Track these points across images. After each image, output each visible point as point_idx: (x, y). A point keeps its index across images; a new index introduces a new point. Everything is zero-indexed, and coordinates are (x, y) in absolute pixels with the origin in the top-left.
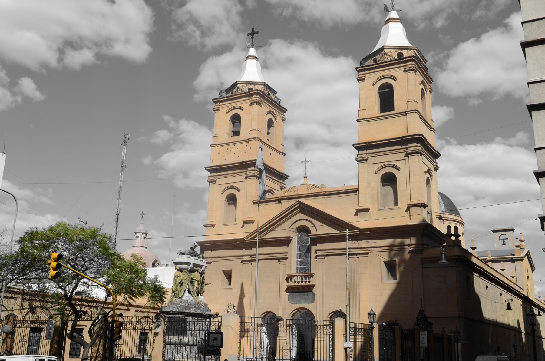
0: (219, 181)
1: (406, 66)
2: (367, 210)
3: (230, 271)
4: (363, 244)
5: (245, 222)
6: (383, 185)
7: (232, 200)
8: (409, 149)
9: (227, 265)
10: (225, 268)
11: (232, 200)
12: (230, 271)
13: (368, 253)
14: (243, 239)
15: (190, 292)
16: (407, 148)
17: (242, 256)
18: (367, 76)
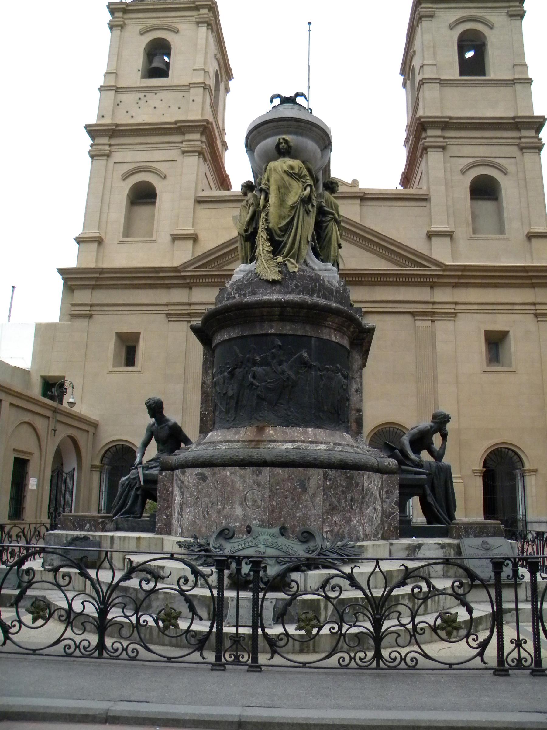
0: (118, 156)
1: (509, 7)
2: (449, 235)
3: (136, 336)
4: (442, 295)
5: (175, 238)
6: (472, 199)
7: (143, 195)
8: (523, 140)
9: (128, 324)
10: (125, 329)
11: (143, 195)
12: (136, 336)
13: (455, 314)
14: (176, 267)
15: (317, 255)
16: (520, 138)
17: (167, 305)
18: (438, 13)
